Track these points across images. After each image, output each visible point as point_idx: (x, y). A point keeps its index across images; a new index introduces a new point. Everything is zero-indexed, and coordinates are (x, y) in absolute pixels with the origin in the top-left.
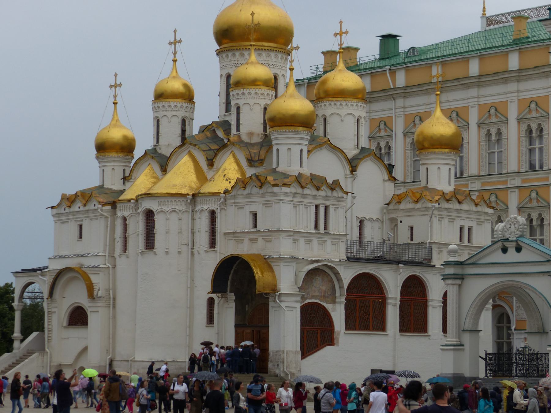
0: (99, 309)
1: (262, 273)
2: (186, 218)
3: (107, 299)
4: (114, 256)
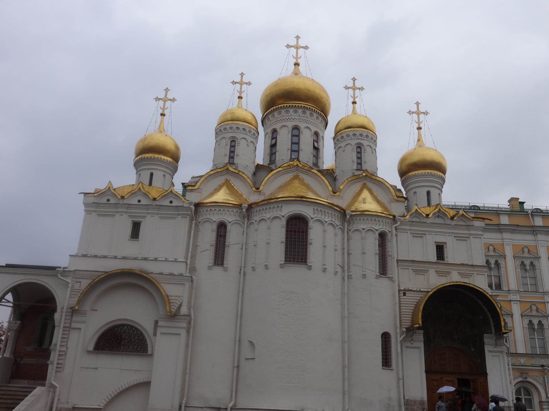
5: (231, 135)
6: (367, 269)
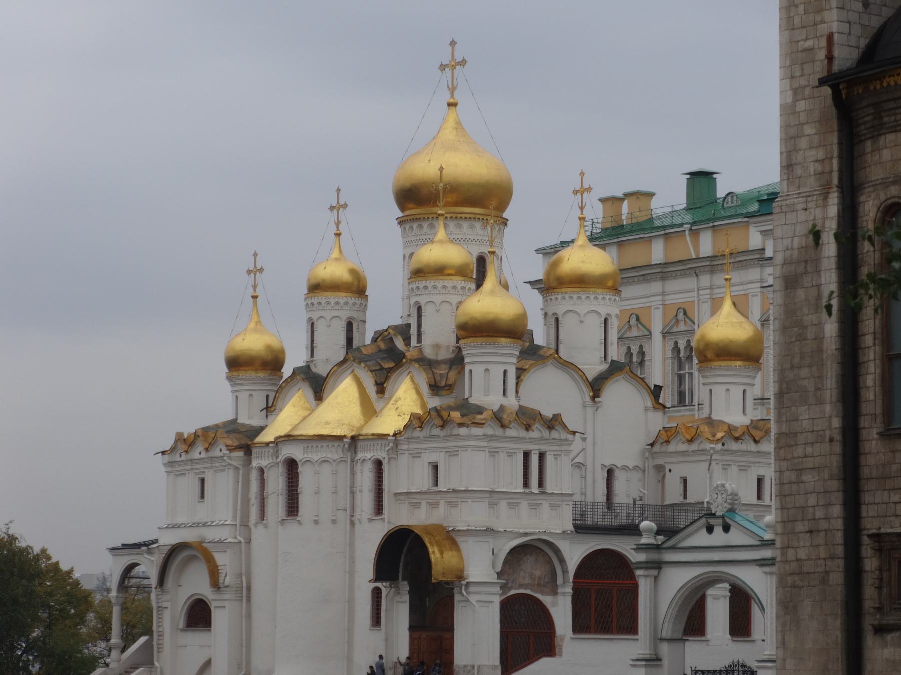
0: (226, 604)
1: (442, 553)
2: (344, 471)
3: (238, 589)
4: (248, 526)
6: (363, 511)
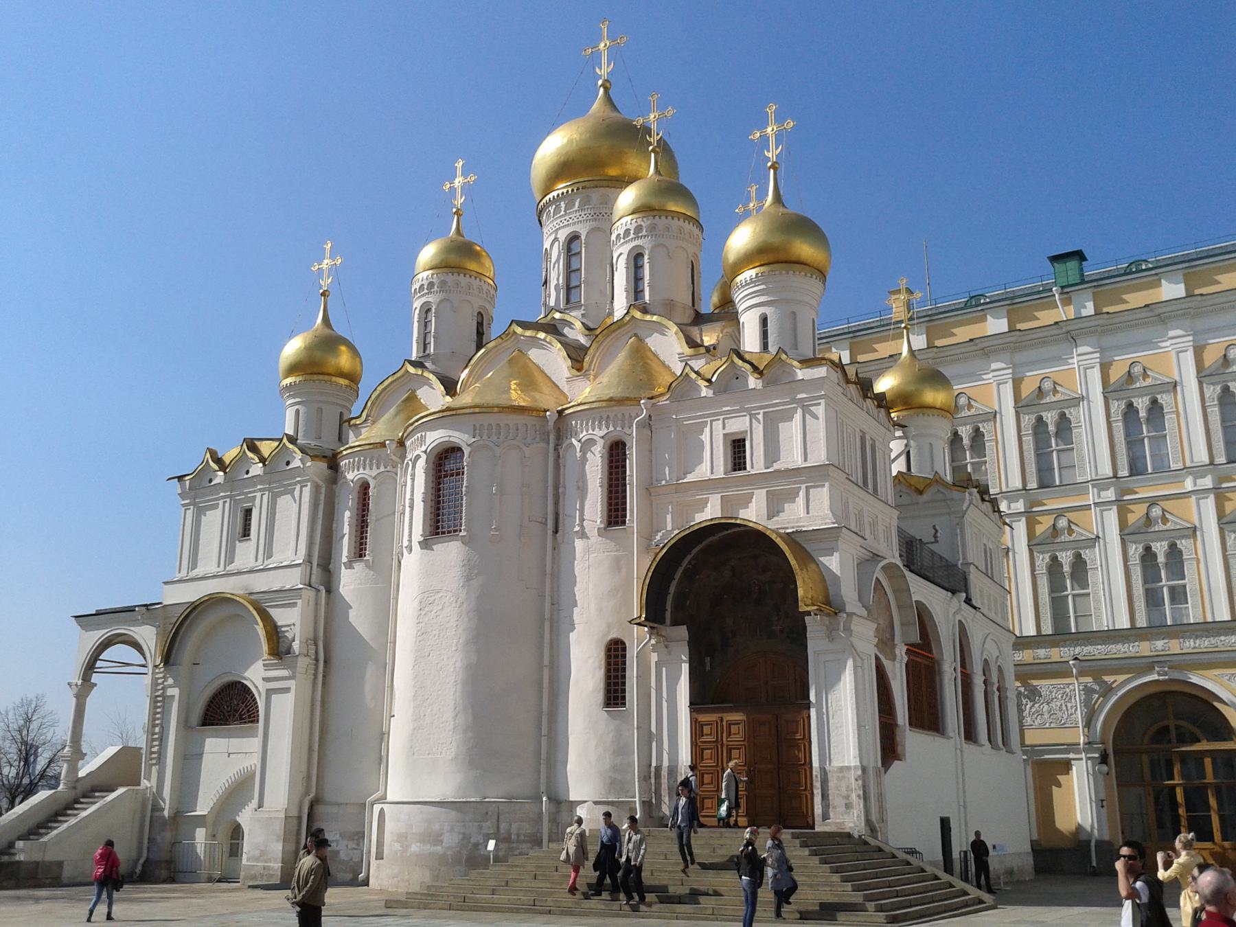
0: (292, 684)
5: (424, 300)
